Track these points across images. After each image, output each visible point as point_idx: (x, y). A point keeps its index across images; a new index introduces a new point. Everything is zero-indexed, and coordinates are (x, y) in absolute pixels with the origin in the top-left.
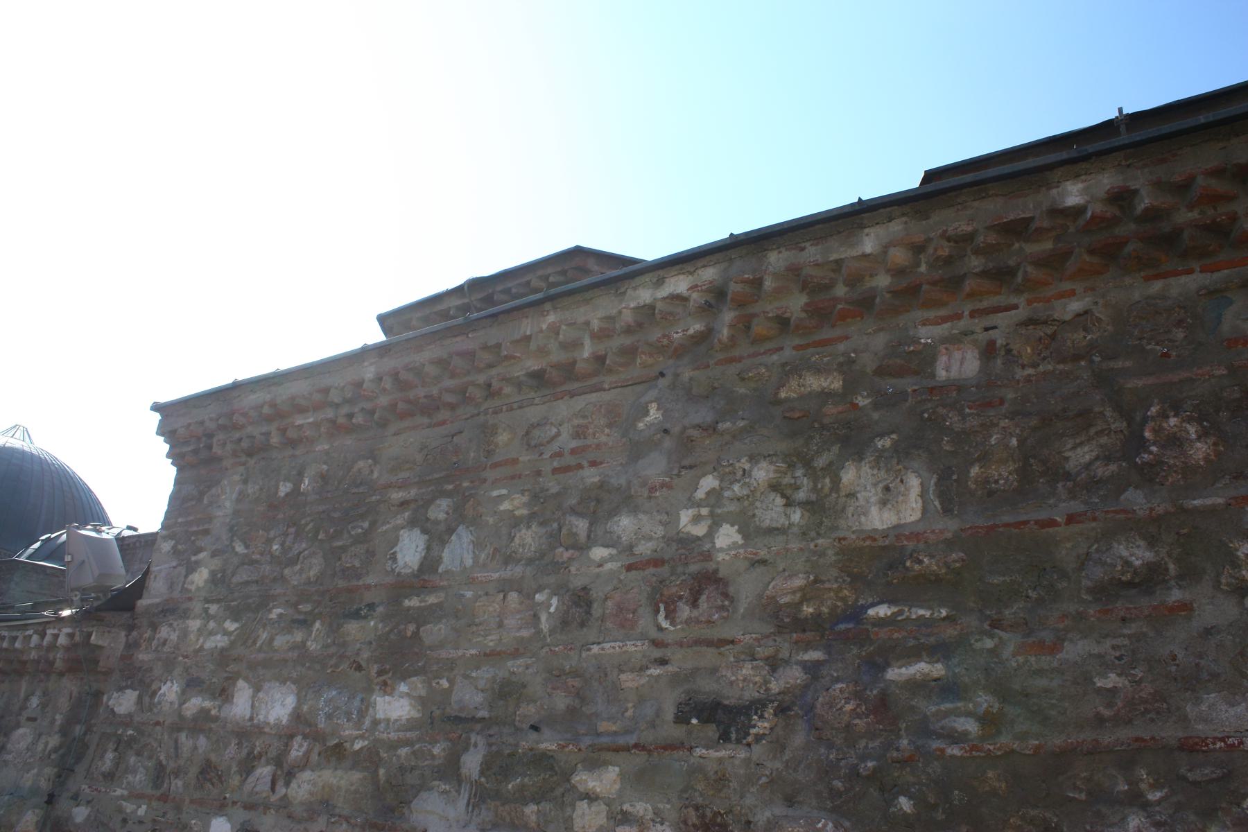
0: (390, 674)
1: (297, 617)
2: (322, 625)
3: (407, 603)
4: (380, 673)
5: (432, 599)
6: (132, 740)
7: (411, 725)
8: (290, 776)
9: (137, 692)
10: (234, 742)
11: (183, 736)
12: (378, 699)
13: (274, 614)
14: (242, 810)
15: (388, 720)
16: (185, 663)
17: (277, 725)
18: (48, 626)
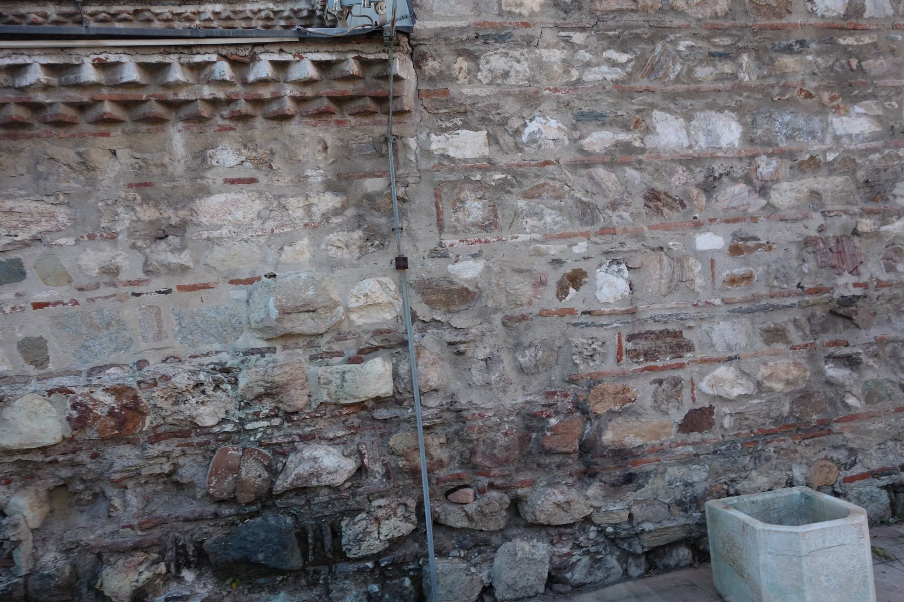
0: (840, 100)
1: (713, 50)
2: (749, 57)
3: (841, 41)
4: (832, 99)
5: (867, 40)
6: (503, 187)
7: (874, 137)
8: (763, 190)
9: (484, 133)
10: (680, 169)
11: (600, 172)
12: (834, 120)
13: (682, 46)
14: (724, 224)
15: (850, 136)
16: (559, 97)
17: (731, 147)
18: (257, 50)
